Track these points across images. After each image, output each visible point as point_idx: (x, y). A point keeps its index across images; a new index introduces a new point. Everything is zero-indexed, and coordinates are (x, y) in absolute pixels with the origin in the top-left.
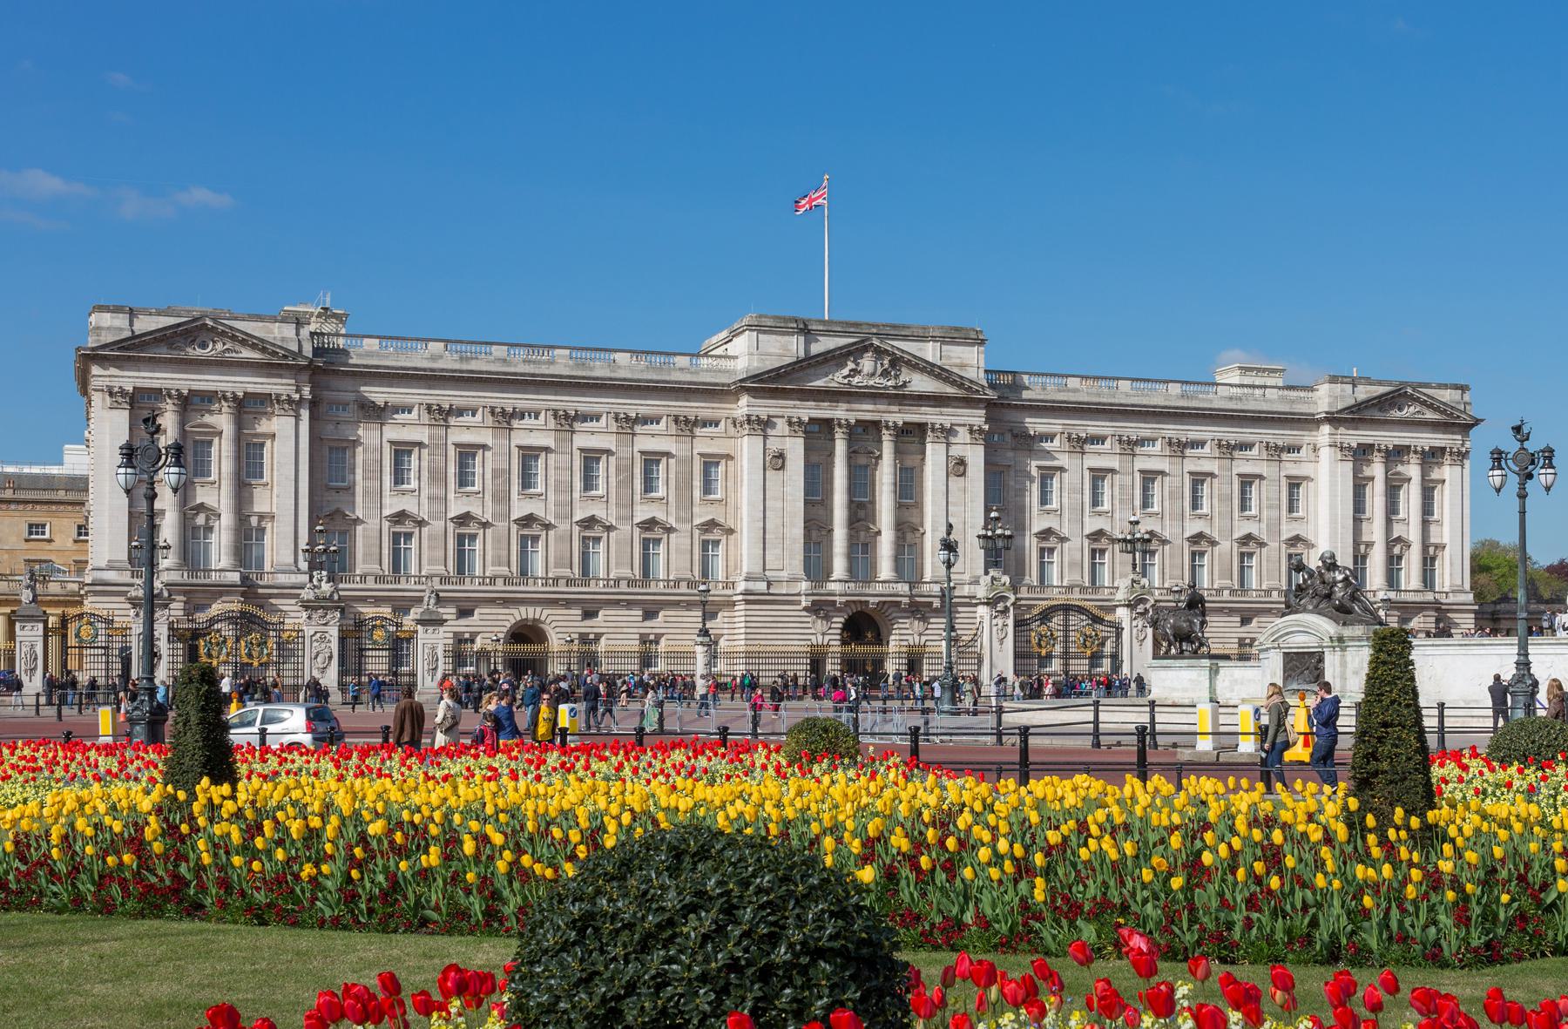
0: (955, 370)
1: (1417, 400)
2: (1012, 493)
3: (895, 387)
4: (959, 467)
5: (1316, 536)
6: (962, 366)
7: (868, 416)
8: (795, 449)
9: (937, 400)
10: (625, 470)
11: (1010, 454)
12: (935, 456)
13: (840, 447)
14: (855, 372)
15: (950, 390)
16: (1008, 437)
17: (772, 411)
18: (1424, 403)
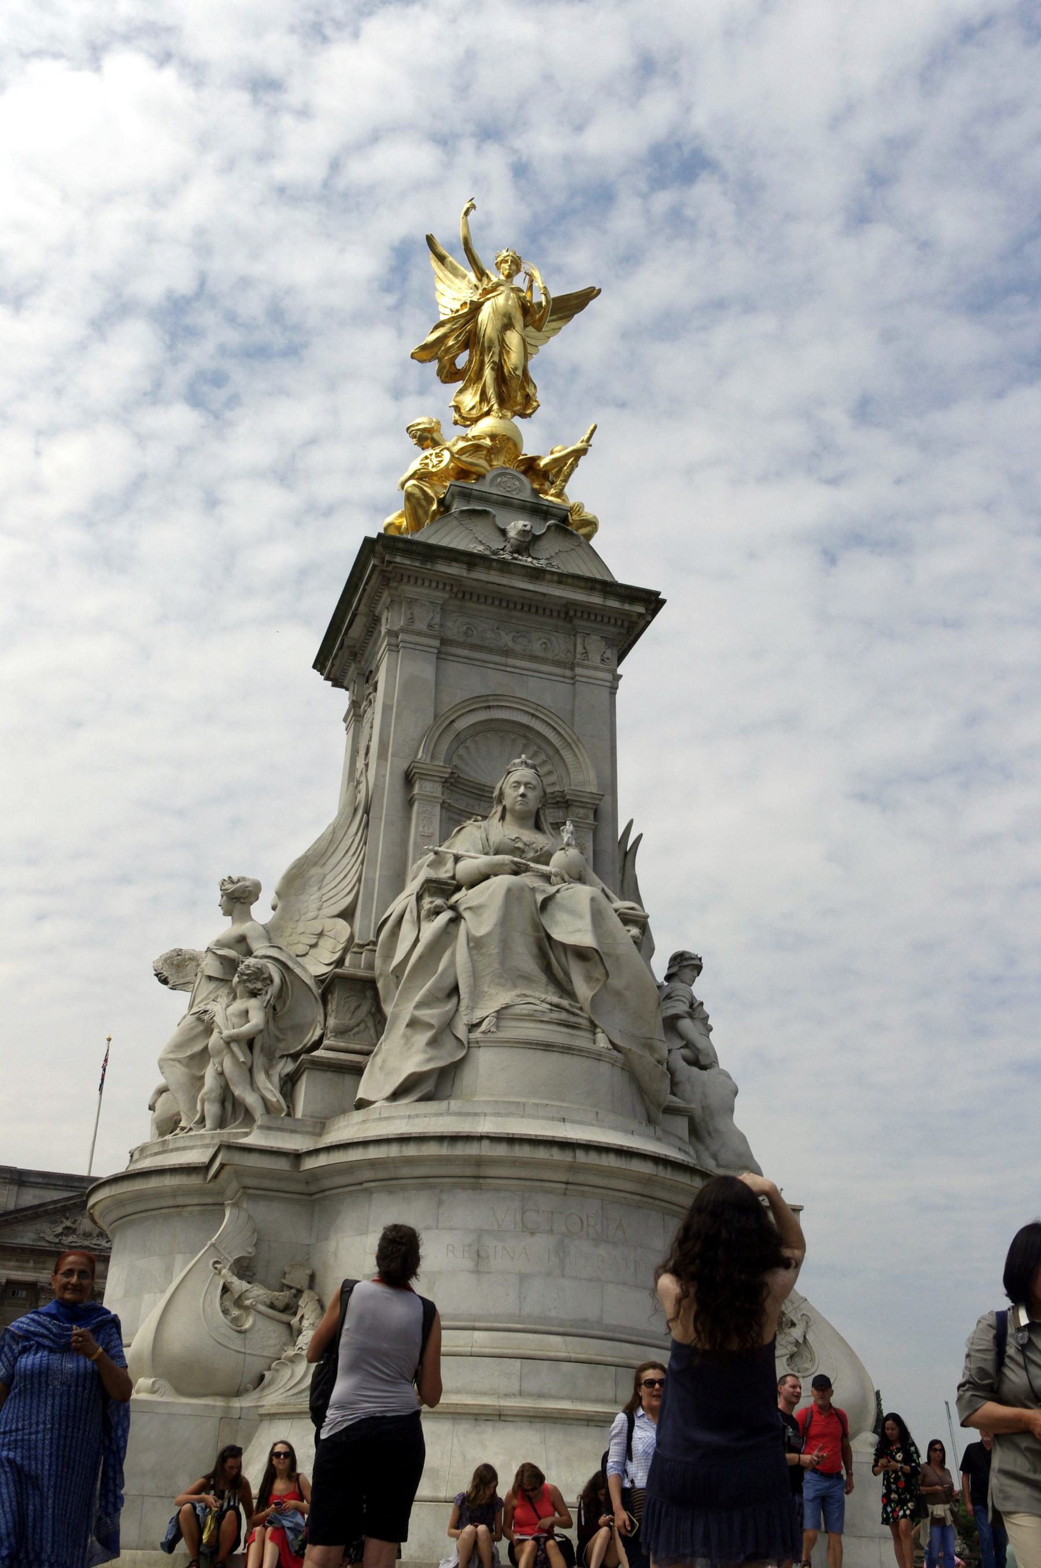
14: (69, 1231)
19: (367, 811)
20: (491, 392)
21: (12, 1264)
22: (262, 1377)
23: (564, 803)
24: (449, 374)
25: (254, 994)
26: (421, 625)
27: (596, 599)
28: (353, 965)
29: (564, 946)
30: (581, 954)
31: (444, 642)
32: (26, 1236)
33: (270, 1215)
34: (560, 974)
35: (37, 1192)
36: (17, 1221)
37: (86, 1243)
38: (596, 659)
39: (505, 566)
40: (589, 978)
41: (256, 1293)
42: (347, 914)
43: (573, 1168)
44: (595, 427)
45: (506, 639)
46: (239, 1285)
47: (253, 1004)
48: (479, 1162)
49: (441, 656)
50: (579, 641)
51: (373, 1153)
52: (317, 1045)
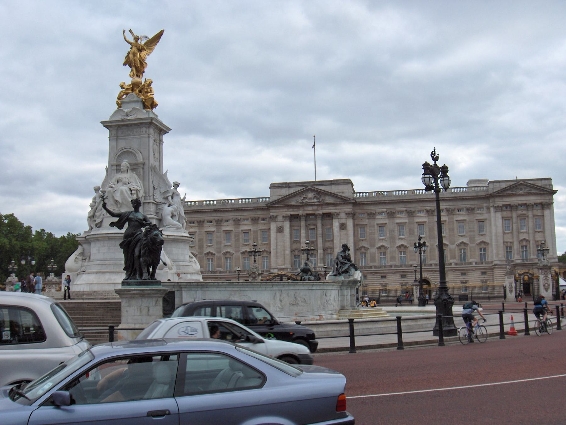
0: (341, 194)
1: (526, 185)
2: (368, 234)
3: (319, 202)
4: (343, 226)
5: (491, 240)
6: (343, 193)
7: (311, 212)
8: (287, 225)
9: (334, 204)
10: (237, 236)
11: (367, 220)
12: (336, 224)
13: (303, 223)
14: (305, 198)
15: (338, 201)
16: (366, 215)
17: (278, 214)
18: (529, 186)
20: (135, 72)
21: (291, 210)
23: (137, 164)
24: (130, 66)
26: (113, 135)
31: (117, 137)
32: (293, 202)
33: (85, 246)
35: (294, 188)
36: (289, 198)
37: (310, 201)
38: (144, 132)
39: (123, 121)
41: (80, 258)
43: (108, 237)
45: (129, 132)
48: (97, 237)
49: (117, 140)
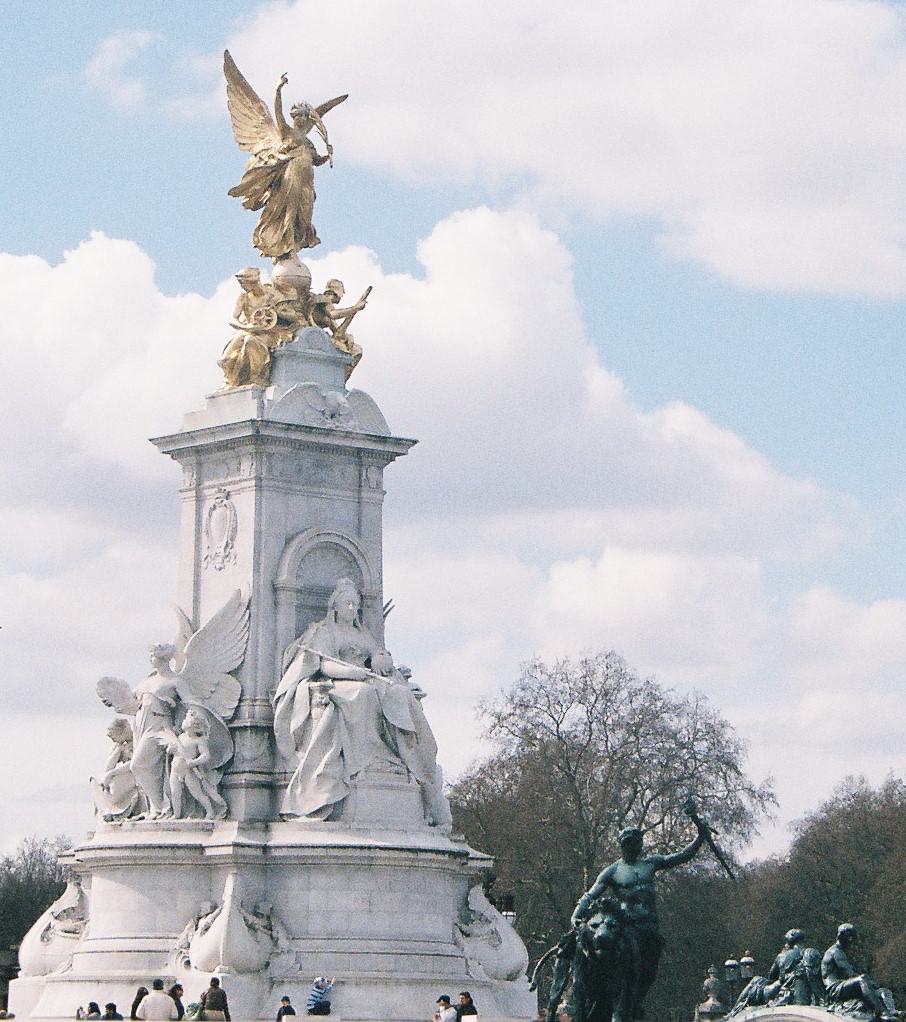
19: (248, 608)
22: (268, 964)
25: (199, 735)
27: (380, 447)
28: (252, 716)
29: (394, 726)
30: (403, 731)
34: (390, 739)
40: (409, 746)
41: (259, 923)
42: (235, 673)
44: (371, 288)
46: (251, 919)
47: (198, 740)
50: (364, 471)
51: (314, 852)
52: (231, 762)
